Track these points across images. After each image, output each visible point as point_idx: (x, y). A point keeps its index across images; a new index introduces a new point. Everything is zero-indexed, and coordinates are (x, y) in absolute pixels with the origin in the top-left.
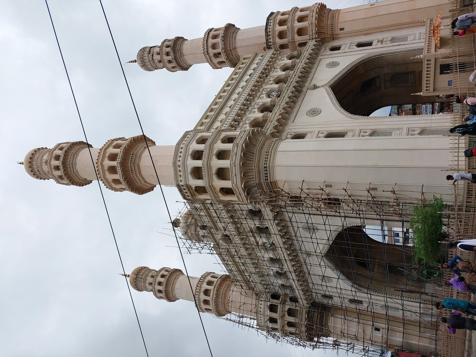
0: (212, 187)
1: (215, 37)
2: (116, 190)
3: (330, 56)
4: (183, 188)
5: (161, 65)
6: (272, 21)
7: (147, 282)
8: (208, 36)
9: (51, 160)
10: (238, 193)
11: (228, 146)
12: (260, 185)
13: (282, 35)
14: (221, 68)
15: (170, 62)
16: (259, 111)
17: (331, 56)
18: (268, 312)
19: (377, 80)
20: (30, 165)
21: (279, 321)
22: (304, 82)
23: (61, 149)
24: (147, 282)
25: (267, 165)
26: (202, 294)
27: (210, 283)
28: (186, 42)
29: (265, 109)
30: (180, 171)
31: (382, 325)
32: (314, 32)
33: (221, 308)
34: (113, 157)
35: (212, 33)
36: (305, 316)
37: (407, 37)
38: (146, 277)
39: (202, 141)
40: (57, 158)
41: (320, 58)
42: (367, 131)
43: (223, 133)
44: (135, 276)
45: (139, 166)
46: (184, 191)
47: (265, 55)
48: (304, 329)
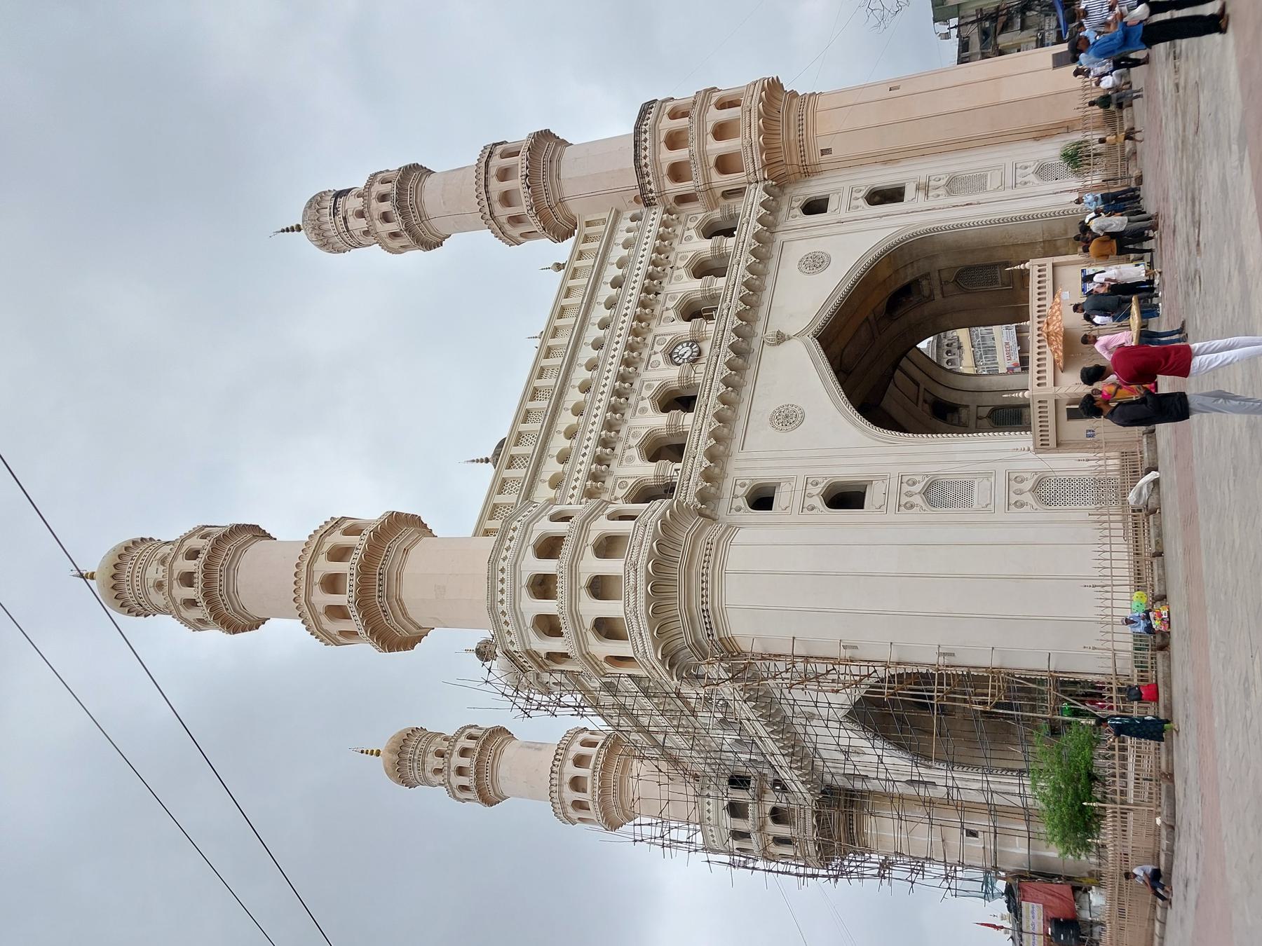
1: (504, 175)
3: (803, 235)
6: (647, 135)
12: (697, 646)
13: (677, 173)
15: (394, 235)
17: (809, 234)
18: (728, 822)
19: (924, 283)
21: (753, 835)
24: (429, 768)
26: (567, 788)
27: (580, 761)
31: (980, 822)
32: (758, 165)
36: (811, 821)
38: (424, 756)
41: (780, 237)
45: (399, 601)
48: (811, 848)
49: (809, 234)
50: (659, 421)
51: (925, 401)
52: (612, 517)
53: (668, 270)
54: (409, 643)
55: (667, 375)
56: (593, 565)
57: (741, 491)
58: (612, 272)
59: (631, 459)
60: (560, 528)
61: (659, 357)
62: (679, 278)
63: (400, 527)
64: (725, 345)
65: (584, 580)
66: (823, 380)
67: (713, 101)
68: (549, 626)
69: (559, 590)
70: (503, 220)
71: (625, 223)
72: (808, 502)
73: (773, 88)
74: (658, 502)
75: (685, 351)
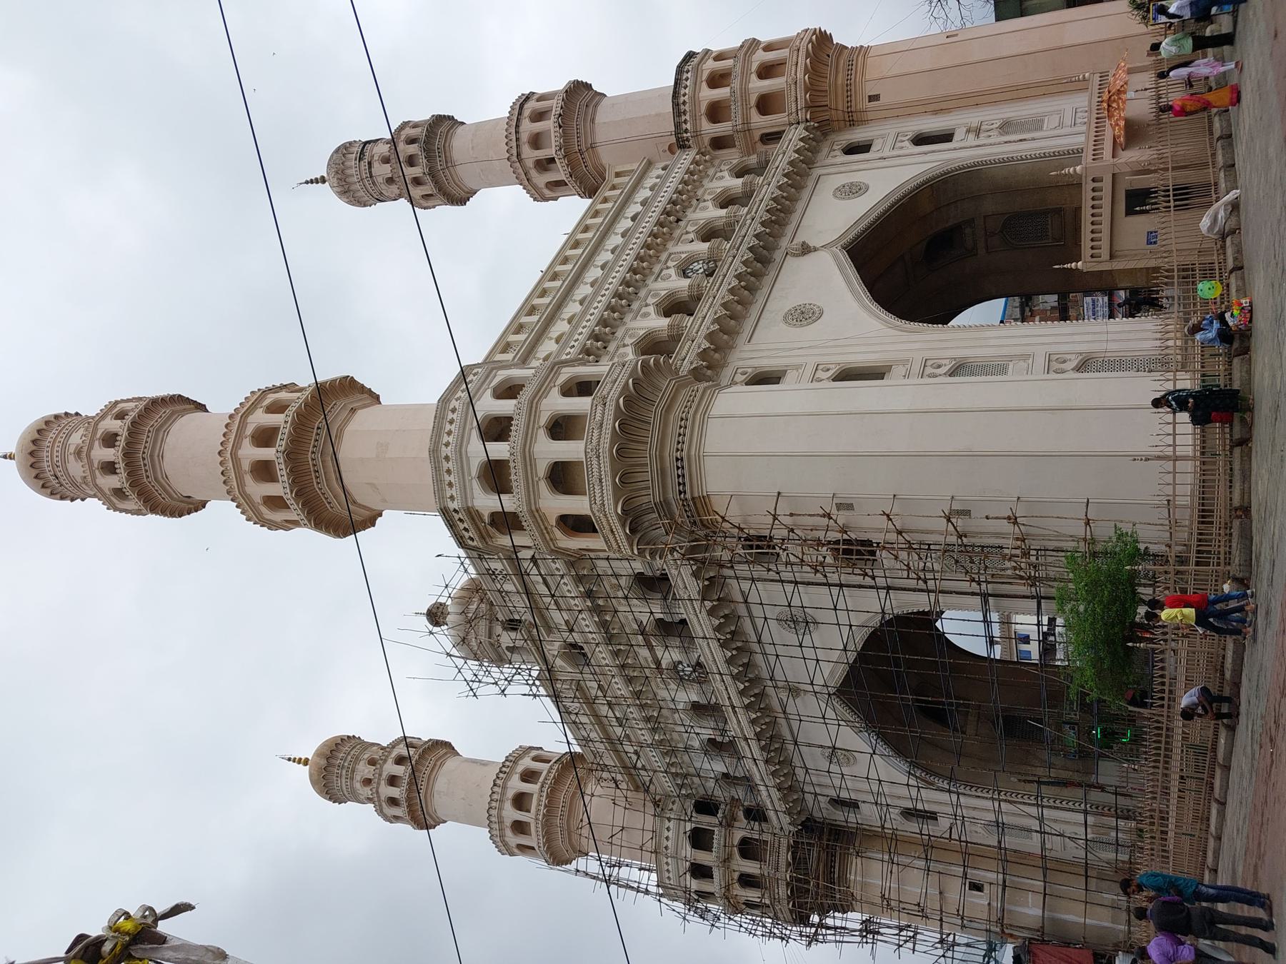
0: (536, 514)
1: (539, 116)
2: (272, 526)
3: (843, 169)
4: (456, 516)
5: (394, 189)
7: (358, 778)
8: (520, 114)
9: (91, 447)
10: (607, 527)
11: (580, 404)
12: (664, 507)
13: (716, 112)
14: (556, 199)
15: (417, 182)
16: (658, 313)
18: (688, 851)
19: (968, 231)
20: (33, 460)
21: (716, 873)
22: (776, 236)
23: (121, 416)
24: (358, 778)
26: (508, 806)
27: (529, 776)
28: (460, 129)
29: (675, 307)
30: (449, 472)
31: (989, 876)
32: (801, 104)
33: (560, 843)
34: (265, 437)
35: (531, 106)
36: (785, 856)
37: (1043, 121)
38: (355, 763)
39: (509, 391)
40: (110, 440)
41: (816, 172)
42: (943, 362)
43: (564, 370)
44: (323, 762)
46: (461, 526)
47: (674, 165)
48: (783, 891)
49: (848, 169)
55: (676, 284)
66: (848, 283)
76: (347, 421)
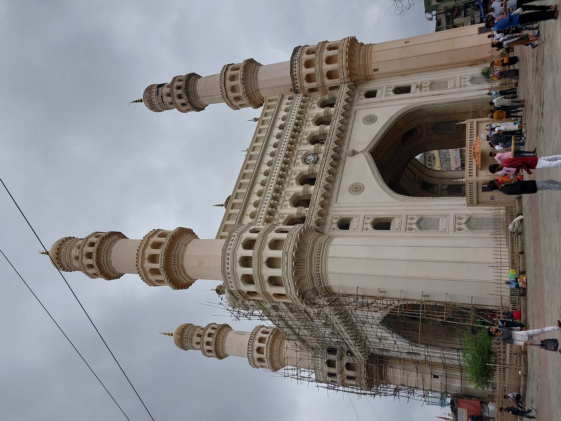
1: (233, 78)
3: (365, 107)
5: (173, 106)
12: (314, 290)
13: (309, 78)
15: (183, 104)
17: (368, 106)
18: (327, 369)
19: (419, 129)
21: (338, 375)
24: (194, 342)
25: (320, 272)
26: (255, 352)
27: (261, 340)
31: (440, 372)
32: (346, 75)
36: (364, 369)
37: (447, 82)
41: (355, 108)
44: (179, 337)
45: (183, 267)
48: (364, 381)
49: (368, 106)
50: (299, 189)
51: (418, 182)
52: (277, 231)
53: (305, 122)
54: (186, 286)
56: (269, 253)
57: (335, 221)
58: (280, 122)
59: (286, 206)
60: (255, 236)
61: (300, 161)
62: (309, 125)
63: (184, 234)
64: (329, 155)
65: (264, 259)
67: (326, 46)
68: (248, 279)
69: (253, 264)
70: (232, 98)
71: (286, 101)
72: (365, 226)
73: (353, 41)
74: (298, 225)
75: (311, 158)
76: (185, 250)
